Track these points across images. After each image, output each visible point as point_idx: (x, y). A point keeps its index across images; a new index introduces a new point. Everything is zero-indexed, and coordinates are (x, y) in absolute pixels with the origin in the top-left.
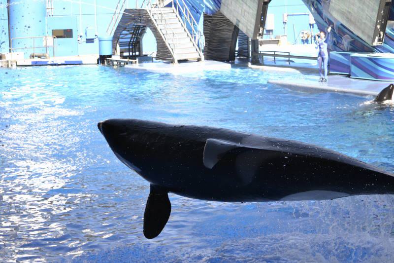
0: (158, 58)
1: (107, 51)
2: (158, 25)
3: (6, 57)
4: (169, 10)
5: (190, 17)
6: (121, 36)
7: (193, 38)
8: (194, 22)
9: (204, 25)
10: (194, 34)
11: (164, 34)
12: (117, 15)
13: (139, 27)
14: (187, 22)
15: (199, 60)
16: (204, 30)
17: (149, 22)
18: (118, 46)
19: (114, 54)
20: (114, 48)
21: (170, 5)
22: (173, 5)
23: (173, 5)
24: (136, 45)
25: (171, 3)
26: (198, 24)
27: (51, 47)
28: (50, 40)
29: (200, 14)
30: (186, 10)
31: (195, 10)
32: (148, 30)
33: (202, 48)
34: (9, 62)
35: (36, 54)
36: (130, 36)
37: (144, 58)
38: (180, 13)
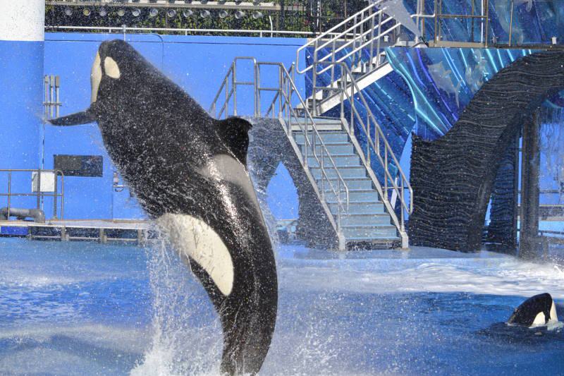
0: (299, 234)
2: (304, 157)
4: (332, 125)
7: (386, 194)
9: (413, 164)
10: (390, 185)
11: (317, 182)
15: (397, 244)
16: (411, 176)
21: (334, 113)
22: (342, 114)
23: (342, 114)
25: (340, 105)
26: (399, 160)
27: (48, 194)
28: (48, 181)
29: (405, 137)
30: (372, 126)
31: (394, 128)
32: (281, 170)
33: (406, 216)
35: (14, 210)
38: (358, 132)
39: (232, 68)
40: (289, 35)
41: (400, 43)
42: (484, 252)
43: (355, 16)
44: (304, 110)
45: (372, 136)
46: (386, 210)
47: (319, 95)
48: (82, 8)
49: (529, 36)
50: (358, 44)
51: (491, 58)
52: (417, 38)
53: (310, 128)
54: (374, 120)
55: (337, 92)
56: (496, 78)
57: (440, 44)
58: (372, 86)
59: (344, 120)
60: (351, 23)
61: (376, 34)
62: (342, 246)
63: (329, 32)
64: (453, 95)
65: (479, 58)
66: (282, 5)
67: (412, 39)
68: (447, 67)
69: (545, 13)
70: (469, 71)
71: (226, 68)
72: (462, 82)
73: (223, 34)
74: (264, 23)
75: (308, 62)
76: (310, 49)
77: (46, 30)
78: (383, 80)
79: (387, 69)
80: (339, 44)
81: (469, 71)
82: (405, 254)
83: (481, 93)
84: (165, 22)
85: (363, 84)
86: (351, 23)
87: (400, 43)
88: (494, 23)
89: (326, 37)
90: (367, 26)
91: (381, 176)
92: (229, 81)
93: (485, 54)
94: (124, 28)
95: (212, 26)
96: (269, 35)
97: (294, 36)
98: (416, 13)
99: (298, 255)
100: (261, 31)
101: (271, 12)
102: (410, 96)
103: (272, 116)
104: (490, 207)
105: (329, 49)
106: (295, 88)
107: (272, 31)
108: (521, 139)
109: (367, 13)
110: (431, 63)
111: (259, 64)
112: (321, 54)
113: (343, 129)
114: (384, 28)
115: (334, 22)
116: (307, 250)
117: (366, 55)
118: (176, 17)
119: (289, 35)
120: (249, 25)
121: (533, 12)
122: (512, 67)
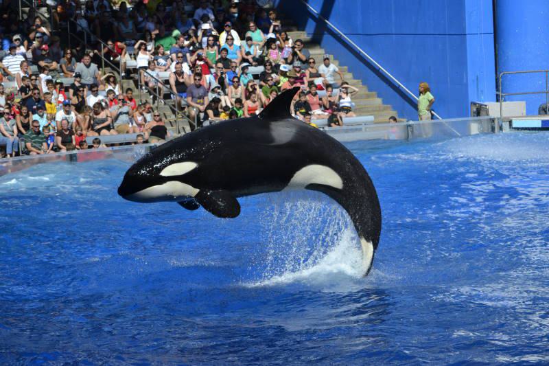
3: (490, 112)
34: (496, 122)
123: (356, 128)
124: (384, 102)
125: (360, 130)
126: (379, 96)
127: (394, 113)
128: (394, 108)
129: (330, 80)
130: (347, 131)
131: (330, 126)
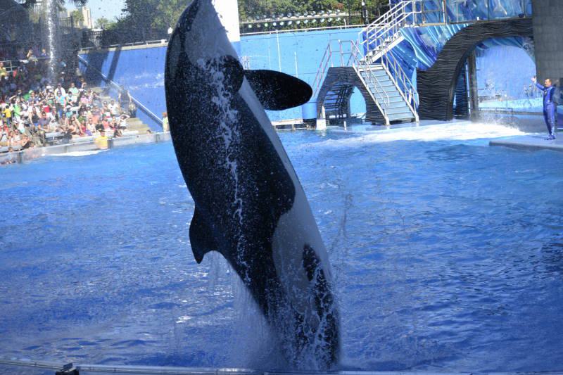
0: (367, 120)
1: (311, 116)
4: (378, 67)
5: (402, 74)
6: (327, 97)
8: (406, 79)
9: (417, 82)
10: (407, 92)
12: (320, 74)
13: (346, 86)
14: (398, 79)
15: (413, 120)
17: (356, 81)
18: (323, 109)
19: (319, 117)
20: (319, 111)
21: (378, 61)
22: (382, 62)
23: (382, 62)
24: (343, 106)
25: (380, 58)
29: (413, 70)
30: (397, 66)
31: (406, 65)
32: (356, 90)
36: (336, 97)
37: (355, 121)
38: (390, 70)
39: (329, 45)
40: (354, 27)
41: (406, 26)
42: (454, 120)
43: (384, 15)
44: (364, 62)
45: (397, 70)
46: (407, 104)
47: (370, 54)
48: (256, 24)
49: (466, 17)
50: (387, 28)
51: (449, 29)
52: (414, 23)
53: (368, 69)
54: (397, 63)
55: (379, 51)
56: (453, 38)
57: (425, 25)
58: (395, 47)
59: (383, 64)
60: (382, 19)
61: (394, 22)
62: (388, 123)
63: (372, 24)
64: (433, 48)
65: (444, 30)
66: (350, 13)
67: (412, 24)
68: (429, 35)
69: (472, 6)
70: (440, 36)
71: (326, 46)
72: (437, 41)
73: (323, 29)
74: (342, 23)
75: (364, 38)
76: (365, 33)
77: (241, 36)
78: (400, 44)
79: (402, 38)
80: (378, 29)
81: (440, 36)
82: (417, 124)
83: (445, 47)
84: (295, 26)
85: (390, 47)
86: (382, 19)
87: (406, 26)
88: (449, 12)
89: (372, 26)
90: (390, 19)
91: (403, 89)
92: (328, 51)
93: (446, 28)
94: (277, 31)
95: (318, 27)
96: (344, 28)
97: (356, 27)
98: (412, 11)
99: (367, 129)
100: (341, 27)
101: (345, 17)
102: (413, 50)
103: (350, 65)
104: (455, 99)
105: (373, 32)
106: (359, 51)
107: (346, 26)
108: (467, 66)
109: (390, 14)
110: (421, 34)
111: (341, 42)
112: (370, 34)
113: (383, 69)
114: (398, 19)
115: (374, 20)
116: (371, 127)
117: (391, 33)
118: (300, 24)
119: (354, 27)
120: (335, 24)
121: (467, 6)
122: (459, 33)
123: (129, 137)
124: (144, 123)
125: (131, 138)
126: (141, 120)
127: (148, 128)
128: (149, 126)
129: (114, 112)
130: (124, 139)
131: (115, 137)
